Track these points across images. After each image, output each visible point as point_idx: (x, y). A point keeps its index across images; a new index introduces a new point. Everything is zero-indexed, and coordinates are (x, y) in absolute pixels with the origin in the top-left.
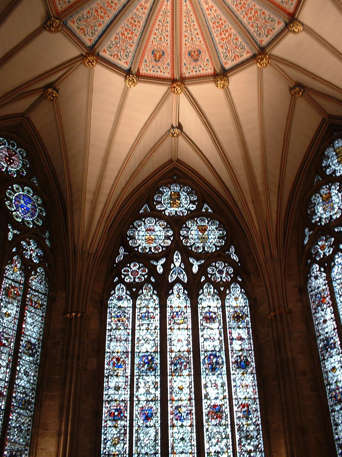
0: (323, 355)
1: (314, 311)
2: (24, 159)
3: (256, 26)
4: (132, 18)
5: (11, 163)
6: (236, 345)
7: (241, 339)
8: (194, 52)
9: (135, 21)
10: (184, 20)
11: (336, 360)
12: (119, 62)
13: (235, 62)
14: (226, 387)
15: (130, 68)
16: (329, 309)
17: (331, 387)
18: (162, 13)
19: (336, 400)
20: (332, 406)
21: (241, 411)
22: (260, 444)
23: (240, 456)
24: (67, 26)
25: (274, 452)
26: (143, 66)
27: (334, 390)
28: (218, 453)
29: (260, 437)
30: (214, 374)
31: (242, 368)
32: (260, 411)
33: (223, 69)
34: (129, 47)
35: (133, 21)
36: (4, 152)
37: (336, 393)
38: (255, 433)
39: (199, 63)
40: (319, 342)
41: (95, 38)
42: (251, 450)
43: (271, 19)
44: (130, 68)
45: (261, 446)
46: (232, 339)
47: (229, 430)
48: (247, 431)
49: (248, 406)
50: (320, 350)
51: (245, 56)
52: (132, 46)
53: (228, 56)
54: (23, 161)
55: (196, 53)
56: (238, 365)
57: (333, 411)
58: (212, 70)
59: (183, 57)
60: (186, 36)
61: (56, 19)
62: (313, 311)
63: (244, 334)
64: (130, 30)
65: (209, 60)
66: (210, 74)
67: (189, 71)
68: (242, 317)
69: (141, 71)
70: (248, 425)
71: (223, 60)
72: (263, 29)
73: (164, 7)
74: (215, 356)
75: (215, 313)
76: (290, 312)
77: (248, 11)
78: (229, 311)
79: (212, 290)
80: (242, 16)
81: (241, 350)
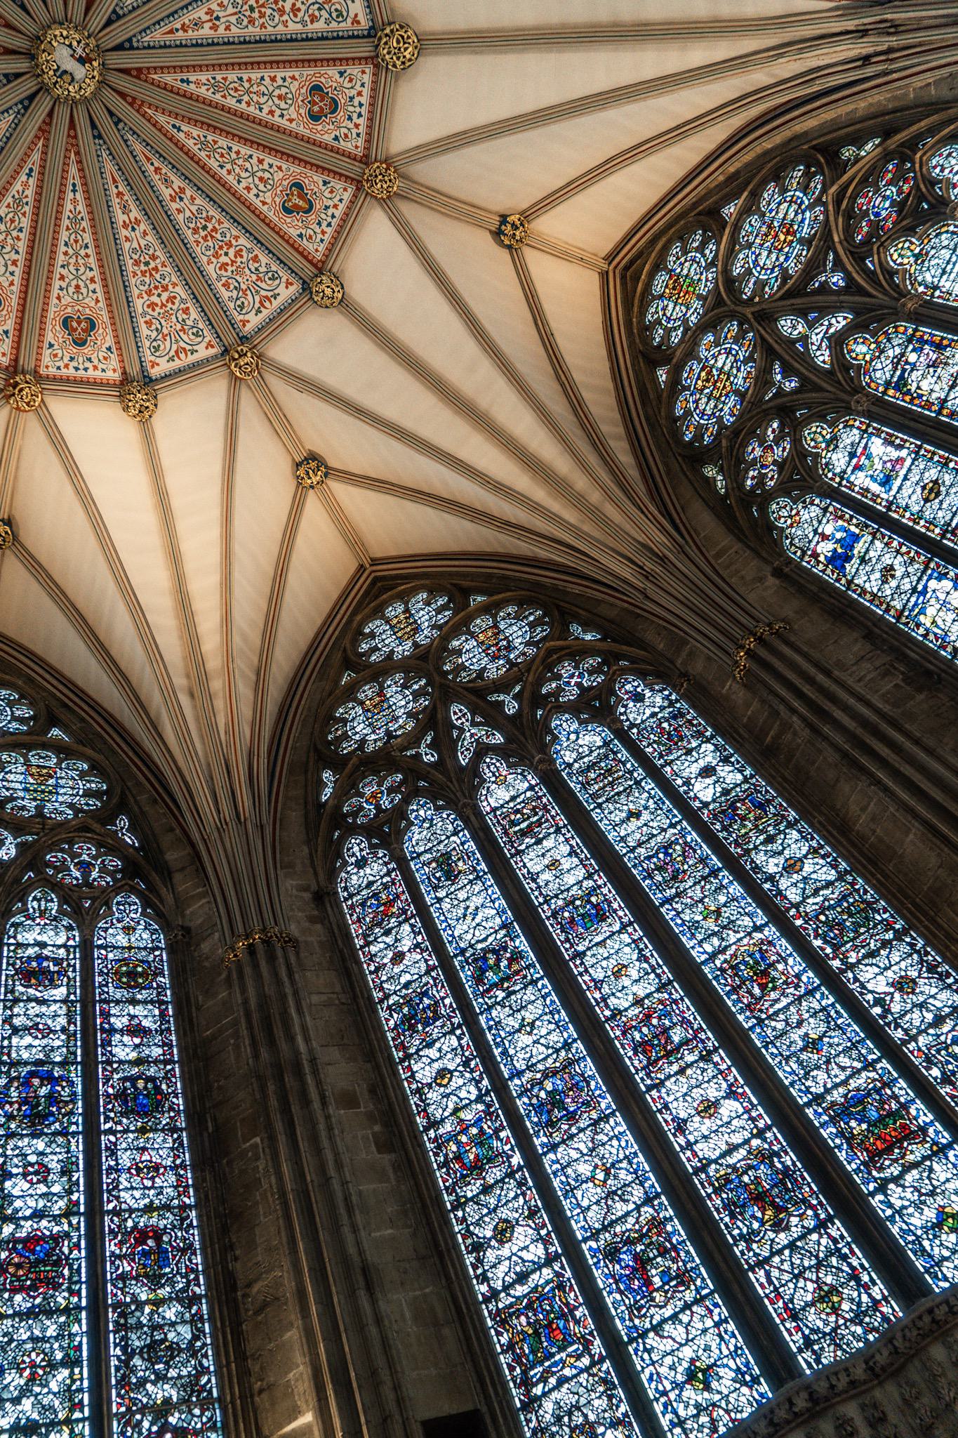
0: (403, 1047)
1: (362, 942)
6: (124, 1049)
7: (135, 1030)
8: (79, 323)
10: (64, 235)
11: (445, 1048)
14: (79, 1176)
16: (406, 928)
17: (441, 1131)
19: (463, 1166)
20: (451, 1190)
21: (133, 1253)
22: (203, 1370)
23: (123, 1433)
25: (261, 1391)
27: (453, 1137)
28: (32, 1427)
29: (205, 1345)
30: (34, 1135)
31: (139, 1115)
32: (203, 1249)
37: (458, 1143)
38: (186, 1332)
39: (87, 350)
40: (383, 1014)
42: (167, 1401)
45: (210, 1381)
46: (112, 1031)
47: (80, 1328)
48: (155, 1327)
49: (157, 1234)
50: (389, 1035)
53: (162, 347)
55: (83, 325)
56: (125, 1102)
57: (458, 1205)
59: (49, 327)
60: (62, 278)
62: (359, 942)
63: (147, 1017)
65: (114, 349)
67: (58, 364)
68: (144, 974)
70: (158, 1303)
72: (250, 297)
74: (49, 1079)
75: (57, 961)
76: (292, 941)
77: (221, 248)
78: (105, 959)
79: (54, 906)
80: (205, 259)
81: (138, 1062)
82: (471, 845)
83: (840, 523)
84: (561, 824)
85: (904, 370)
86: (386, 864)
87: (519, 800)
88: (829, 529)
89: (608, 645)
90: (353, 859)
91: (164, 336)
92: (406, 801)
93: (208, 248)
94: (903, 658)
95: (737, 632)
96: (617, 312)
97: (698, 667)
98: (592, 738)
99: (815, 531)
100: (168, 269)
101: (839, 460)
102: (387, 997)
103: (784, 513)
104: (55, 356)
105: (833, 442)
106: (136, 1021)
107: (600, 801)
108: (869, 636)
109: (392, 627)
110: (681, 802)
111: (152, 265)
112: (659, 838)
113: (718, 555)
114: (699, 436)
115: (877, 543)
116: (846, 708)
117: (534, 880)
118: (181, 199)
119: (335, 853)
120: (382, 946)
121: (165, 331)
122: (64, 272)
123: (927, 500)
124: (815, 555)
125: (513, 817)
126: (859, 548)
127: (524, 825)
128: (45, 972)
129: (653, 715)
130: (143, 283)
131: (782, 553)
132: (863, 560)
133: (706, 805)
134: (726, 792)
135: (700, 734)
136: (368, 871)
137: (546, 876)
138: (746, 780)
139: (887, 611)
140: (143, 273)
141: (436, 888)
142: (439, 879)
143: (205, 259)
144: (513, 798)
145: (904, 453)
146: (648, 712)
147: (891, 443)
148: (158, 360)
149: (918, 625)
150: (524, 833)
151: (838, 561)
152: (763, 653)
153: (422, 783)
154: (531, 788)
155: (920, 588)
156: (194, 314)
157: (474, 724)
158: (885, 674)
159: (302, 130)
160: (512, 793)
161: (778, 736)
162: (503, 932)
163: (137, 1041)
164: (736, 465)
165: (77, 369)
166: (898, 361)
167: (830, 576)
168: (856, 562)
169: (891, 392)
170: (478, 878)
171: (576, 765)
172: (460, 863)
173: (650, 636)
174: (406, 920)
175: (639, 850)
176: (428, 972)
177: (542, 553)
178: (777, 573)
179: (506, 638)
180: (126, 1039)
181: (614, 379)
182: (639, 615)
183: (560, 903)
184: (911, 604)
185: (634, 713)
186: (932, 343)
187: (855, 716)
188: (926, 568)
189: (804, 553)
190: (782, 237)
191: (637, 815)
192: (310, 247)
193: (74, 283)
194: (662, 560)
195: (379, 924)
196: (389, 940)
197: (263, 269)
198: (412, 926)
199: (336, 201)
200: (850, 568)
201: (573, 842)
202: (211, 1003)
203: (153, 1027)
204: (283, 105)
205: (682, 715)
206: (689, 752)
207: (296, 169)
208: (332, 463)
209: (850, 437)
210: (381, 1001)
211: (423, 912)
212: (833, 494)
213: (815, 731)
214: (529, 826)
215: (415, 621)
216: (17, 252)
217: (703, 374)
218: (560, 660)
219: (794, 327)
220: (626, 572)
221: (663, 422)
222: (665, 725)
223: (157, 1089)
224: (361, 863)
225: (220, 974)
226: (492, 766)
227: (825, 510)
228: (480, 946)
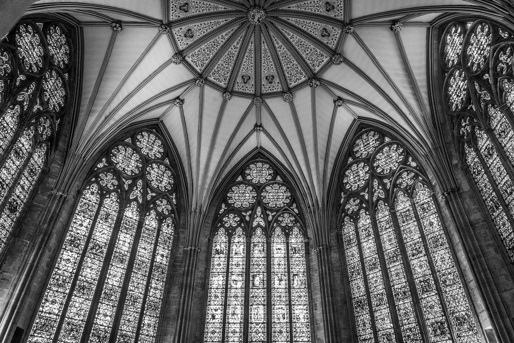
8: (191, 33)
82: (115, 218)
83: (225, 248)
84: (133, 235)
85: (257, 245)
86: (97, 200)
87: (132, 220)
88: (222, 246)
89: (175, 207)
90: (92, 190)
91: (198, 56)
92: (113, 191)
93: (225, 59)
94: (205, 280)
95: (193, 243)
96: (250, 157)
97: (182, 236)
98: (154, 224)
99: (221, 243)
100: (216, 51)
101: (237, 240)
102: (72, 231)
103: (222, 232)
104: (179, 31)
105: (239, 236)
106: (24, 185)
107: (143, 239)
108: (206, 269)
109: (148, 141)
110: (154, 256)
111: (215, 46)
112: (144, 259)
113: (206, 222)
114: (230, 198)
115: (224, 259)
116: (191, 278)
117: (119, 241)
118: (235, 48)
119: (90, 183)
120: (80, 218)
121: (199, 56)
122: (203, 24)
123: (235, 265)
124: (216, 246)
125: (127, 222)
126: (221, 255)
127: (127, 226)
128: (19, 154)
129: (166, 233)
130: (209, 45)
131: (213, 238)
132: (219, 257)
133: (156, 262)
134: (161, 263)
135: (168, 247)
136: (92, 197)
137: (120, 242)
138: (165, 265)
139: (212, 269)
140: (212, 45)
141: (101, 219)
142: (103, 218)
143: (222, 59)
144: (131, 218)
145: (242, 254)
146: (167, 231)
147: (243, 250)
148: (190, 58)
149: (212, 277)
150: (126, 228)
151: (218, 252)
152: (193, 252)
153: (119, 190)
154: (136, 220)
155: (219, 273)
156: (207, 62)
157: (140, 191)
158: (200, 279)
159: (263, 75)
160: (132, 217)
161: (177, 265)
162: (104, 244)
163: (21, 191)
164: (227, 213)
165: (178, 38)
166: (259, 242)
167: (214, 252)
168: (219, 256)
169: (253, 244)
170: (110, 227)
171: (146, 226)
172: (110, 219)
173: (182, 218)
174: (89, 219)
175: (139, 257)
176: (84, 236)
177: (187, 175)
178: (209, 240)
179: (163, 179)
180: (20, 188)
181: (234, 166)
182: (185, 211)
183: (118, 251)
184: (215, 273)
185: (164, 228)
186: (264, 248)
187: (191, 281)
188: (223, 272)
189: (215, 243)
190: (276, 197)
191: (145, 250)
192: (236, 86)
193: (201, 28)
194: (200, 213)
195: (84, 213)
196: (83, 219)
198: (90, 222)
199: (249, 89)
200: (217, 256)
201: (131, 241)
202: (41, 196)
203: (26, 189)
204: (267, 69)
205: (170, 240)
206: (164, 248)
207: (253, 76)
208: (184, 106)
209: (241, 240)
210: (70, 231)
211: (95, 221)
212: (230, 243)
213: (184, 274)
214: (128, 228)
215: (153, 147)
216: (203, 11)
217: (243, 191)
218: (166, 199)
219: (259, 212)
220: (194, 206)
221: (229, 186)
222: (166, 238)
223: (17, 207)
224: (92, 193)
225: (48, 192)
226: (134, 205)
227: (226, 243)
228: (98, 242)
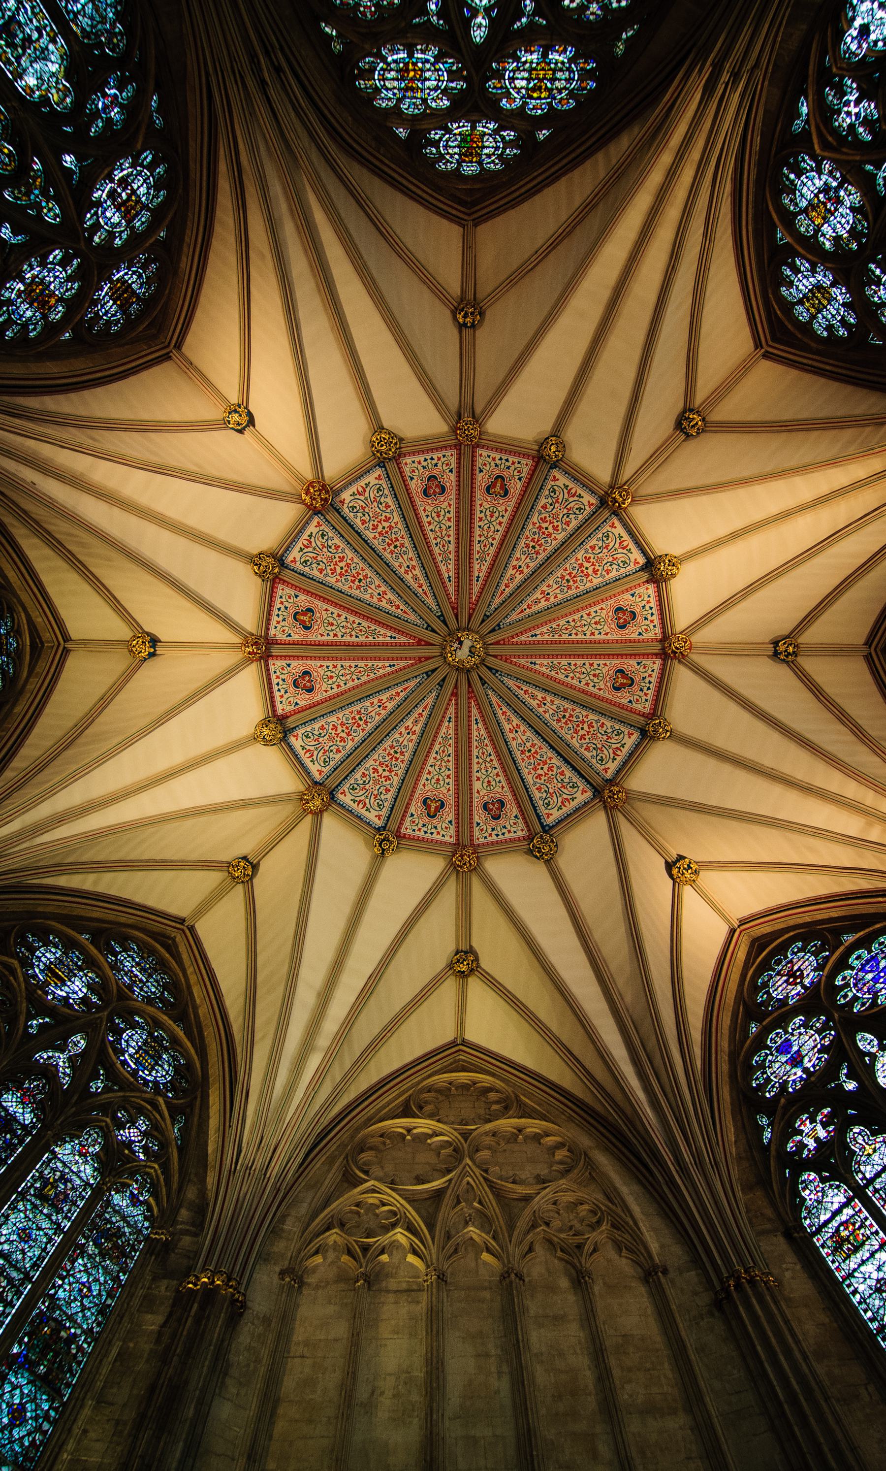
2: (806, 948)
3: (568, 517)
4: (559, 721)
5: (802, 976)
9: (564, 717)
12: (627, 747)
13: (632, 546)
15: (639, 728)
18: (553, 673)
24: (553, 826)
26: (639, 706)
33: (647, 567)
34: (604, 729)
35: (564, 721)
36: (780, 983)
41: (581, 784)
43: (552, 494)
44: (639, 728)
51: (619, 530)
52: (603, 723)
54: (808, 952)
58: (650, 587)
61: (532, 841)
64: (578, 726)
66: (656, 589)
67: (652, 627)
69: (647, 711)
71: (632, 567)
73: (544, 669)
197: (550, 500)
